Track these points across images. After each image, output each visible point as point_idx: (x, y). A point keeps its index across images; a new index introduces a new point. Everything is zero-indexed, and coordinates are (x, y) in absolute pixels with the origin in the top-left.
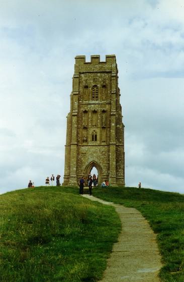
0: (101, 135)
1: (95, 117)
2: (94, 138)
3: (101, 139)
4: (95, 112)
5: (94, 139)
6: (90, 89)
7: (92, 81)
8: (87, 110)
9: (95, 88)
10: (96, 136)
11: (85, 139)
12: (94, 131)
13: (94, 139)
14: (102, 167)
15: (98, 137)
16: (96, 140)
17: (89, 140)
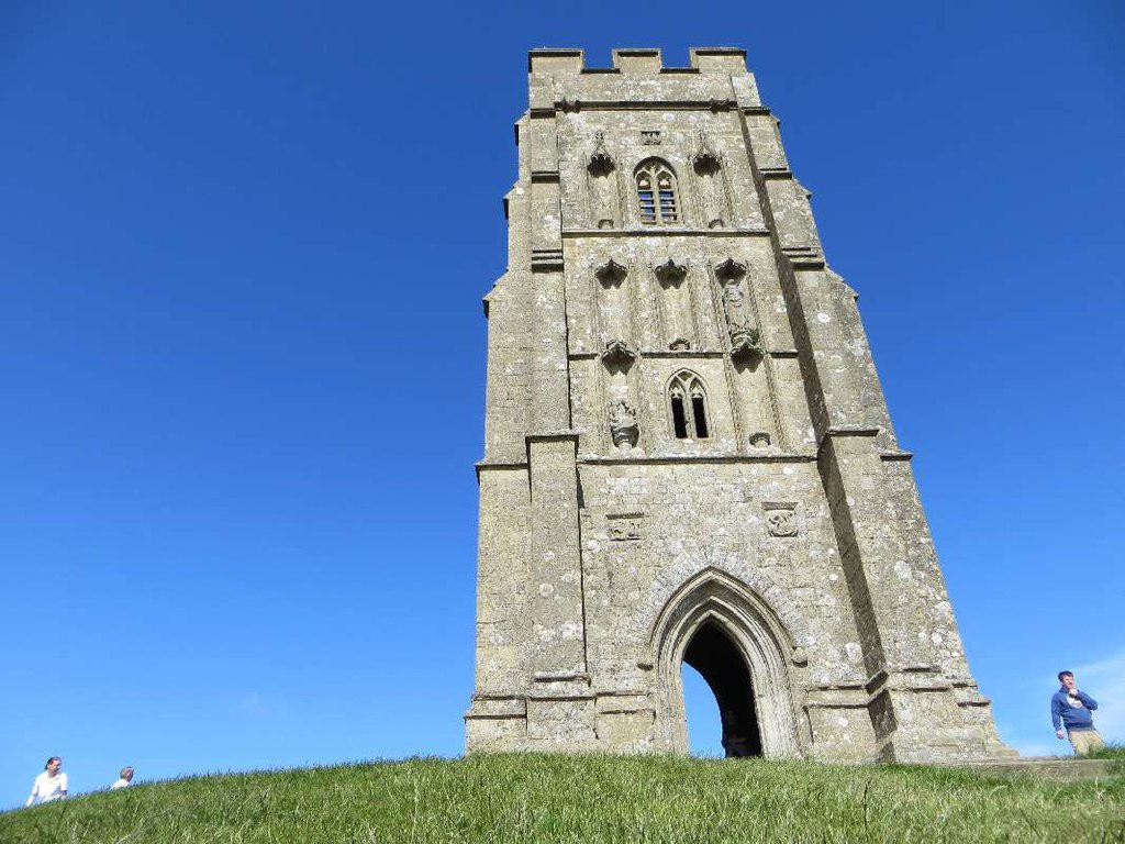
0: (735, 400)
1: (674, 297)
2: (689, 417)
3: (738, 427)
4: (671, 275)
5: (691, 427)
6: (628, 172)
7: (632, 140)
8: (620, 262)
9: (653, 173)
10: (698, 405)
11: (624, 420)
12: (684, 375)
13: (691, 427)
14: (788, 612)
15: (717, 413)
16: (702, 431)
17: (658, 429)
